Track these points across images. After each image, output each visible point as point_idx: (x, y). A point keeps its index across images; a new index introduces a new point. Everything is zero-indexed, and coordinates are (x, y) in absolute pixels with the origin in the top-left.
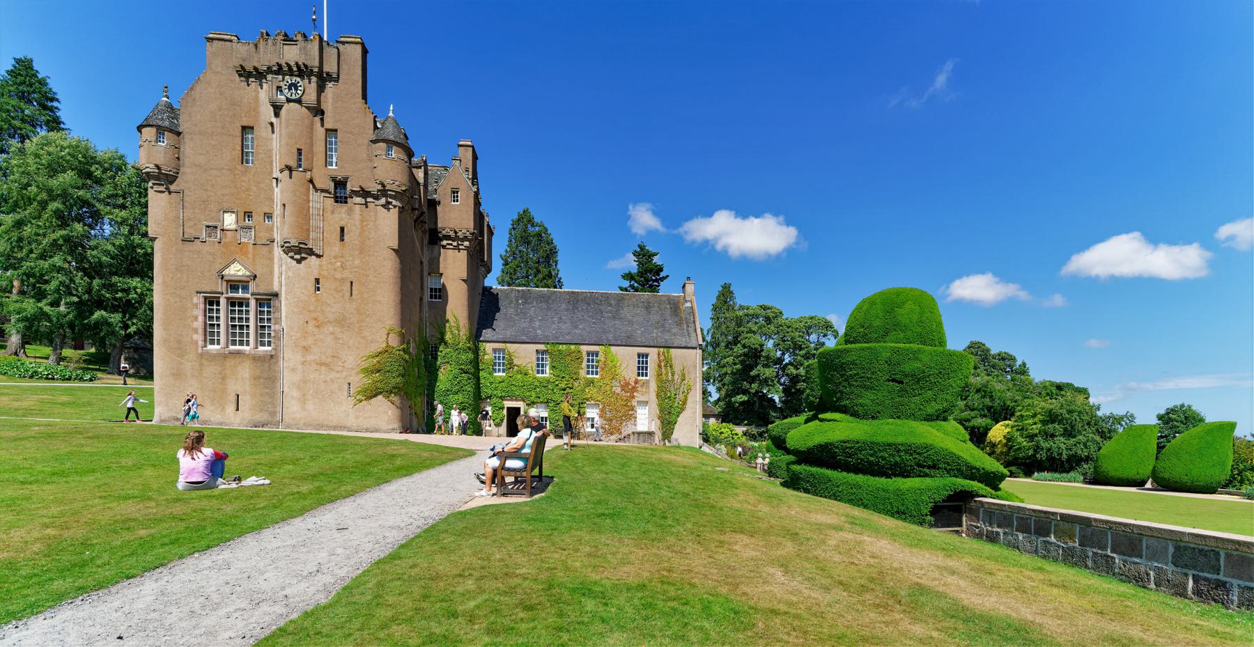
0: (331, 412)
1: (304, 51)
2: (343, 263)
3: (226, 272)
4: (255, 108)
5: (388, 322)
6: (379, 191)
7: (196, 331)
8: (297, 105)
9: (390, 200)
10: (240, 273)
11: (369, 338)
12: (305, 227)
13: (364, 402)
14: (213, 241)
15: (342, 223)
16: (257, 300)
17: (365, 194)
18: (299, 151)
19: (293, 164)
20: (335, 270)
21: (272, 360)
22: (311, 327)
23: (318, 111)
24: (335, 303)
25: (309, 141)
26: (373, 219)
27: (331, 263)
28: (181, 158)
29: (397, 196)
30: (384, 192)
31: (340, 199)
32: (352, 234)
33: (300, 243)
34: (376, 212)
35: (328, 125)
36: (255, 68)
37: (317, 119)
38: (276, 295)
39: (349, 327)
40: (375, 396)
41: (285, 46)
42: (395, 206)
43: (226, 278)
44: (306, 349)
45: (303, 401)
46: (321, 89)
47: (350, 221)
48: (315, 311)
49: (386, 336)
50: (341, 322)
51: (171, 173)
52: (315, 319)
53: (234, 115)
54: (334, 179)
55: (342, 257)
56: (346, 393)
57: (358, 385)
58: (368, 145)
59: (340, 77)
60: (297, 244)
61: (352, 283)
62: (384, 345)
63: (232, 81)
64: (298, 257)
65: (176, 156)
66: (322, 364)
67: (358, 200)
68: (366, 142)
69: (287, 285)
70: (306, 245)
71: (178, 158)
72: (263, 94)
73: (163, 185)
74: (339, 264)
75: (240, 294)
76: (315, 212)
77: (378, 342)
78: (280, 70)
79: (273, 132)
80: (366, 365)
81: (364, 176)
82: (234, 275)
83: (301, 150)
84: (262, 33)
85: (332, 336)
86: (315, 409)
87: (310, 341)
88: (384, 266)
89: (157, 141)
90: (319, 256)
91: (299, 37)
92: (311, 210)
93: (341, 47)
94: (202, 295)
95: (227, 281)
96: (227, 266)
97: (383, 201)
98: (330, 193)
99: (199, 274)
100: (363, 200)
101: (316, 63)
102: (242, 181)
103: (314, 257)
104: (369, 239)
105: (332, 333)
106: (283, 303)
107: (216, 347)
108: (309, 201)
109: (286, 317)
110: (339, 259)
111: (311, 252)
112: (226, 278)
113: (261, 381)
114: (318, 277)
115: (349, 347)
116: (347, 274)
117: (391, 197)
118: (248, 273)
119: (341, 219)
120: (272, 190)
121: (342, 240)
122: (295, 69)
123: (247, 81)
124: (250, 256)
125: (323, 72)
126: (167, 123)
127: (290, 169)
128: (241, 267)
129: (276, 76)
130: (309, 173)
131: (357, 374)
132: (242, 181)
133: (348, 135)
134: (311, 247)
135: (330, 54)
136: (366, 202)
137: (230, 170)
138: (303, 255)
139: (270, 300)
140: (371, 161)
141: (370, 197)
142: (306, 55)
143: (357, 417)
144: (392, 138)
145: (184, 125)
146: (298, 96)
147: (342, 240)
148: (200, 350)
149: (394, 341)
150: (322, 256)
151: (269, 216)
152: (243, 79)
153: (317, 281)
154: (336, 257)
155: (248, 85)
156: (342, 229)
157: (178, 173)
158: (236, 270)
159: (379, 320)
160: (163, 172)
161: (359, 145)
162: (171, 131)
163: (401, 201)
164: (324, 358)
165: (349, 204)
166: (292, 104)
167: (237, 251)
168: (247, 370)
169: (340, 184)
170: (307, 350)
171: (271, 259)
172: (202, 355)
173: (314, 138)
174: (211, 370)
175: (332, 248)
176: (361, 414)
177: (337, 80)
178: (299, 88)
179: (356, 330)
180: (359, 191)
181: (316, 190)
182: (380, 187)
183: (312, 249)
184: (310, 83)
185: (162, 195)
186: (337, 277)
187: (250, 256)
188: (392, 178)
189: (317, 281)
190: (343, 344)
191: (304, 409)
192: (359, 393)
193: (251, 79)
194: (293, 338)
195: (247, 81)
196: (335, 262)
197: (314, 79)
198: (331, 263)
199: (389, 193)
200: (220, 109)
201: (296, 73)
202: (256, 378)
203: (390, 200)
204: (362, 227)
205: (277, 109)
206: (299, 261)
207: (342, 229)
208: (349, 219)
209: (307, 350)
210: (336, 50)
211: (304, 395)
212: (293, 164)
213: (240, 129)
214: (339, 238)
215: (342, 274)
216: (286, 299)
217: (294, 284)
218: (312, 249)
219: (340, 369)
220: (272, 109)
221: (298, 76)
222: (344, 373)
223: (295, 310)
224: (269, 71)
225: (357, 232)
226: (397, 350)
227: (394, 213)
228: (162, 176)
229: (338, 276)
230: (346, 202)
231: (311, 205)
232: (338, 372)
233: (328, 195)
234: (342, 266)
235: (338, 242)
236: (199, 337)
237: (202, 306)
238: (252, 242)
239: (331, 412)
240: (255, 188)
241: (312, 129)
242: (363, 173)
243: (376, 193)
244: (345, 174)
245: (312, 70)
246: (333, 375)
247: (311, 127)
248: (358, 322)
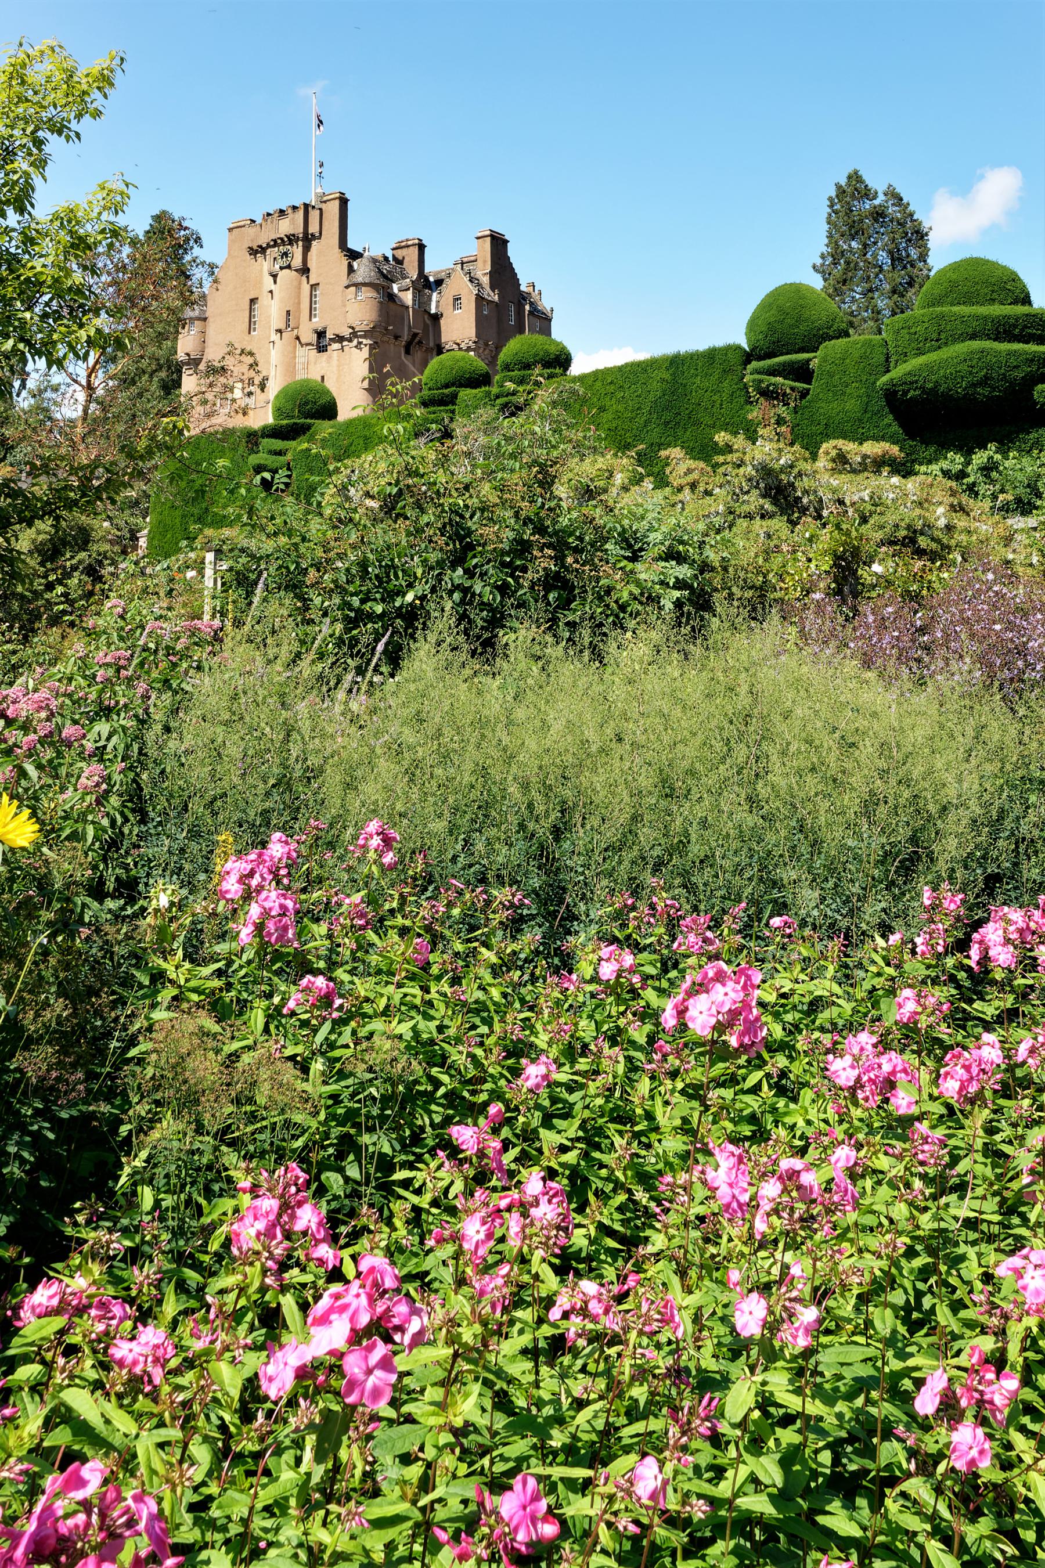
4: (259, 282)
8: (287, 271)
17: (340, 339)
18: (288, 313)
19: (282, 326)
23: (305, 270)
29: (367, 334)
30: (354, 334)
31: (321, 349)
35: (312, 282)
36: (260, 247)
37: (304, 278)
46: (307, 249)
54: (316, 332)
67: (336, 346)
68: (342, 288)
72: (265, 265)
78: (275, 243)
91: (290, 211)
93: (323, 206)
97: (355, 342)
117: (361, 337)
120: (269, 353)
127: (280, 331)
135: (314, 215)
144: (360, 280)
162: (199, 319)
169: (321, 334)
177: (320, 237)
181: (302, 345)
197: (300, 243)
205: (275, 276)
212: (282, 326)
224: (269, 246)
227: (366, 351)
244: (323, 325)
247: (299, 287)
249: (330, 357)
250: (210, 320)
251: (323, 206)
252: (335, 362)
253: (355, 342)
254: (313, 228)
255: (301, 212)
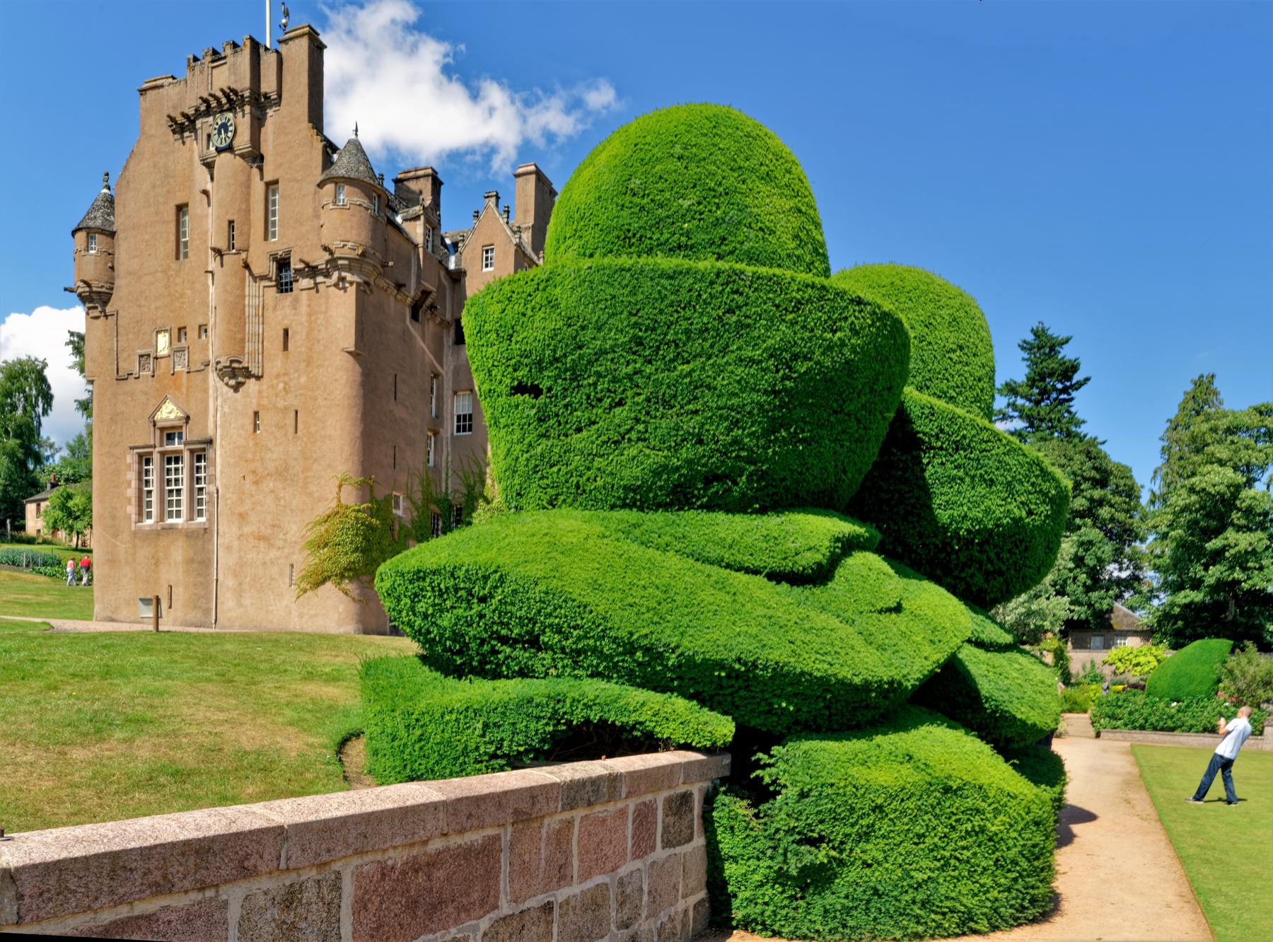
0: (270, 608)
1: (234, 70)
2: (286, 384)
3: (159, 416)
4: (189, 178)
5: (339, 468)
6: (327, 262)
7: (129, 500)
8: (226, 156)
9: (343, 274)
10: (172, 416)
11: (316, 495)
12: (239, 336)
13: (309, 593)
14: (147, 376)
15: (286, 323)
16: (192, 452)
17: (311, 271)
19: (223, 245)
20: (277, 396)
21: (206, 536)
22: (248, 485)
23: (255, 157)
24: (275, 446)
25: (244, 207)
26: (323, 309)
27: (272, 386)
28: (116, 268)
31: (284, 287)
32: (298, 337)
33: (232, 362)
34: (327, 298)
35: (268, 178)
37: (255, 171)
38: (210, 442)
39: (292, 480)
40: (324, 581)
41: (215, 70)
42: (351, 283)
43: (159, 425)
44: (242, 517)
45: (239, 593)
46: (258, 123)
47: (296, 318)
48: (253, 460)
49: (337, 490)
50: (282, 473)
51: (104, 290)
52: (254, 472)
53: (168, 192)
54: (274, 258)
55: (285, 374)
56: (287, 580)
57: (303, 567)
58: (315, 193)
59: (284, 96)
60: (228, 364)
61: (297, 412)
62: (334, 504)
63: (166, 143)
64: (232, 382)
65: (110, 265)
66: (261, 538)
67: (305, 282)
68: (313, 187)
69: (222, 426)
70: (240, 362)
71: (112, 268)
72: (194, 148)
73: (96, 308)
74: (281, 386)
75: (177, 445)
76: (252, 312)
77: (327, 499)
79: (209, 204)
80: (312, 536)
81: (309, 243)
82: (166, 420)
83: (233, 222)
84: (189, 59)
85: (273, 495)
86: (252, 604)
87: (248, 505)
88: (336, 380)
89: (87, 249)
90: (258, 378)
91: (229, 51)
92: (247, 309)
94: (136, 451)
95: (162, 429)
96: (158, 408)
98: (270, 279)
99: (133, 423)
100: (312, 281)
101: (246, 83)
102: (176, 285)
103: (253, 380)
104: (318, 341)
105: (272, 491)
106: (218, 453)
107: (149, 522)
108: (243, 297)
109: (222, 473)
110: (282, 379)
111: (248, 374)
112: (159, 425)
113: (195, 565)
114: (256, 409)
115: (292, 510)
116: (293, 401)
118: (180, 415)
119: (285, 317)
121: (286, 347)
122: (224, 100)
123: (182, 138)
124: (184, 390)
125: (259, 95)
126: (99, 223)
128: (173, 407)
129: (205, 120)
130: (244, 255)
131: (301, 550)
132: (176, 285)
133: (291, 184)
134: (246, 365)
135: (269, 62)
136: (316, 284)
137: (163, 272)
138: (241, 379)
139: (204, 450)
140: (317, 216)
141: (319, 275)
142: (235, 74)
143: (301, 616)
144: (342, 172)
145: (120, 222)
146: (228, 141)
147: (286, 347)
148: (133, 528)
149: (350, 497)
150: (262, 377)
151: (203, 329)
152: (177, 136)
153: (256, 414)
154: (278, 376)
155: (184, 143)
156: (286, 332)
157: (112, 289)
158: (169, 413)
159: (329, 466)
160: (94, 289)
161: (304, 196)
162: (102, 232)
163: (360, 272)
164: (263, 528)
165: (295, 291)
166: (223, 155)
167: (165, 388)
168: (180, 551)
169: (283, 263)
170: (244, 518)
171: (206, 391)
172: (135, 534)
173: (252, 200)
174: (144, 552)
175: (274, 364)
176: (305, 611)
178: (230, 128)
179: (301, 484)
180: (304, 269)
181: (255, 278)
182: (327, 256)
183: (248, 368)
184: (243, 116)
185: (97, 322)
186: (279, 405)
187: (184, 390)
188: (343, 238)
189: (256, 414)
190: (284, 507)
191: (240, 604)
192: (303, 578)
193: (187, 134)
194: (229, 502)
195: (182, 138)
196: (277, 384)
197: (247, 108)
198: (272, 386)
199: (340, 262)
200: (154, 187)
201: (225, 107)
202: (189, 562)
203: (343, 274)
204: (310, 323)
205: (210, 166)
206: (236, 388)
207: (286, 332)
208: (295, 315)
209: (244, 518)
210: (275, 55)
211: (240, 584)
212: (223, 245)
213: (173, 210)
214: (281, 346)
215: (285, 401)
216: (222, 446)
217: (230, 424)
218: (248, 368)
219: (280, 543)
220: (204, 168)
221: (229, 110)
222: (286, 550)
223: (232, 461)
224: (199, 114)
225: (304, 334)
226: (354, 510)
227: (352, 290)
228: (95, 296)
229: (281, 404)
230: (291, 290)
231: (247, 302)
232: (279, 548)
233: (268, 283)
234: (285, 389)
235: (280, 352)
236: (132, 510)
237: (136, 467)
238: (186, 370)
239: (270, 608)
240: (188, 292)
241: (248, 187)
242: (308, 239)
243: (324, 266)
245: (242, 96)
246: (273, 554)
248: (303, 472)
249: (296, 301)
250: (120, 236)
251: (283, 49)
252: (304, 309)
253: (335, 275)
254: (268, 85)
255: (245, 57)
